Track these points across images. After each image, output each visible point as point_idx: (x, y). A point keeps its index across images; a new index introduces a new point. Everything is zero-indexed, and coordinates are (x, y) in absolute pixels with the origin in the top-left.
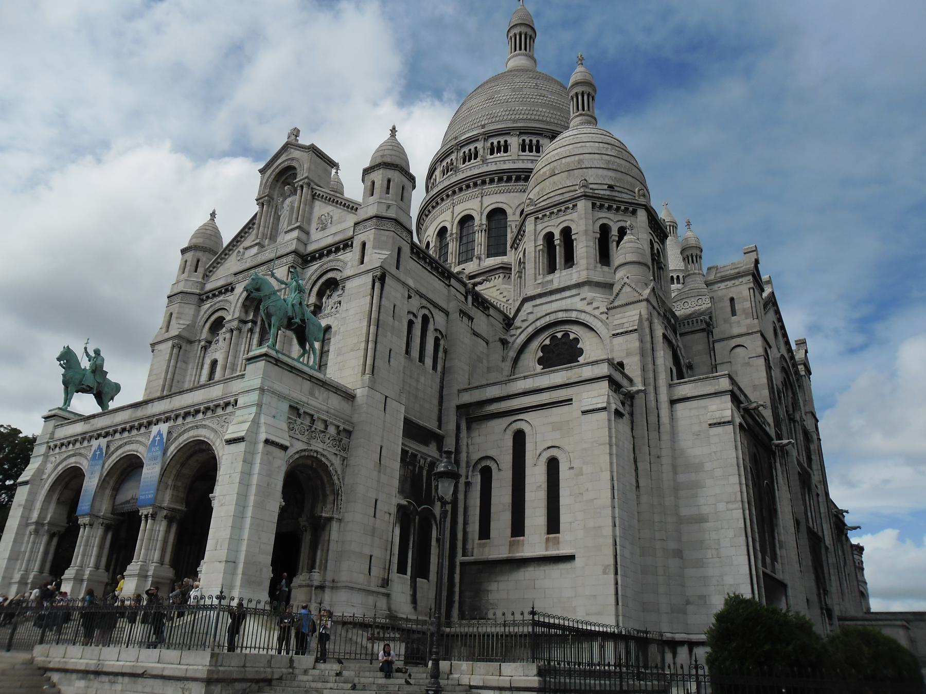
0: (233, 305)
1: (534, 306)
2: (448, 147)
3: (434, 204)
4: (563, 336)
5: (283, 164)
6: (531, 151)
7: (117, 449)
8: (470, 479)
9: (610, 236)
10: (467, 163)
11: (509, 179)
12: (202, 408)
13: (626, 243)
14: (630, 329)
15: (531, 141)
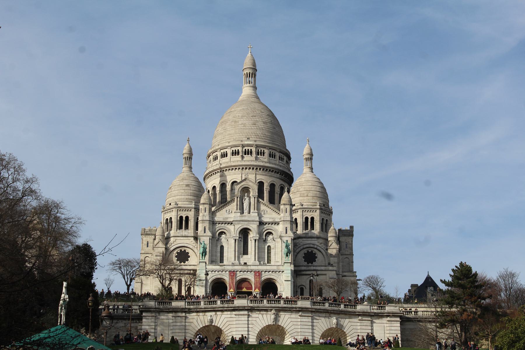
0: (233, 231)
1: (303, 240)
2: (237, 143)
3: (231, 169)
4: (311, 251)
5: (245, 185)
6: (273, 158)
7: (239, 276)
8: (297, 290)
9: (323, 222)
10: (247, 155)
11: (267, 170)
12: (272, 271)
13: (333, 229)
14: (335, 256)
15: (273, 152)
